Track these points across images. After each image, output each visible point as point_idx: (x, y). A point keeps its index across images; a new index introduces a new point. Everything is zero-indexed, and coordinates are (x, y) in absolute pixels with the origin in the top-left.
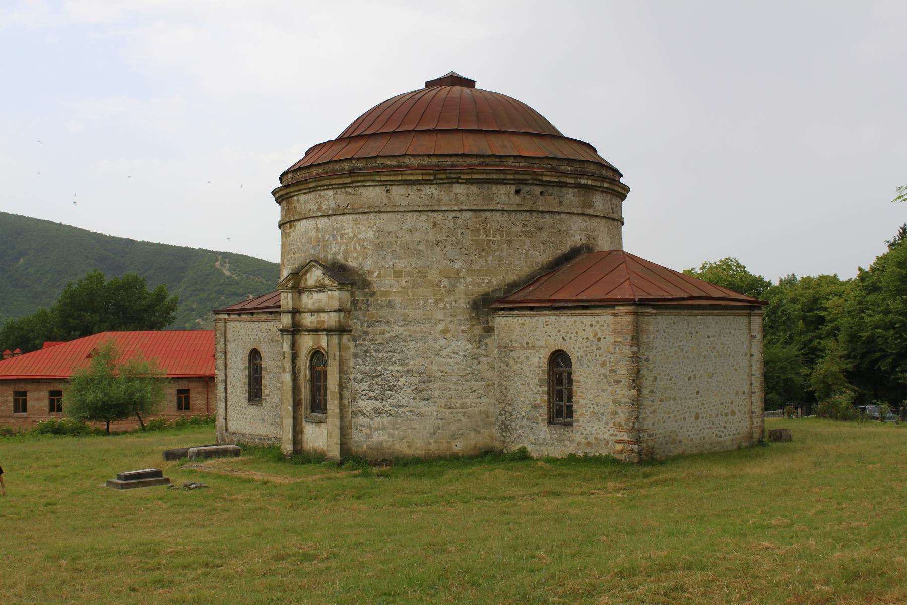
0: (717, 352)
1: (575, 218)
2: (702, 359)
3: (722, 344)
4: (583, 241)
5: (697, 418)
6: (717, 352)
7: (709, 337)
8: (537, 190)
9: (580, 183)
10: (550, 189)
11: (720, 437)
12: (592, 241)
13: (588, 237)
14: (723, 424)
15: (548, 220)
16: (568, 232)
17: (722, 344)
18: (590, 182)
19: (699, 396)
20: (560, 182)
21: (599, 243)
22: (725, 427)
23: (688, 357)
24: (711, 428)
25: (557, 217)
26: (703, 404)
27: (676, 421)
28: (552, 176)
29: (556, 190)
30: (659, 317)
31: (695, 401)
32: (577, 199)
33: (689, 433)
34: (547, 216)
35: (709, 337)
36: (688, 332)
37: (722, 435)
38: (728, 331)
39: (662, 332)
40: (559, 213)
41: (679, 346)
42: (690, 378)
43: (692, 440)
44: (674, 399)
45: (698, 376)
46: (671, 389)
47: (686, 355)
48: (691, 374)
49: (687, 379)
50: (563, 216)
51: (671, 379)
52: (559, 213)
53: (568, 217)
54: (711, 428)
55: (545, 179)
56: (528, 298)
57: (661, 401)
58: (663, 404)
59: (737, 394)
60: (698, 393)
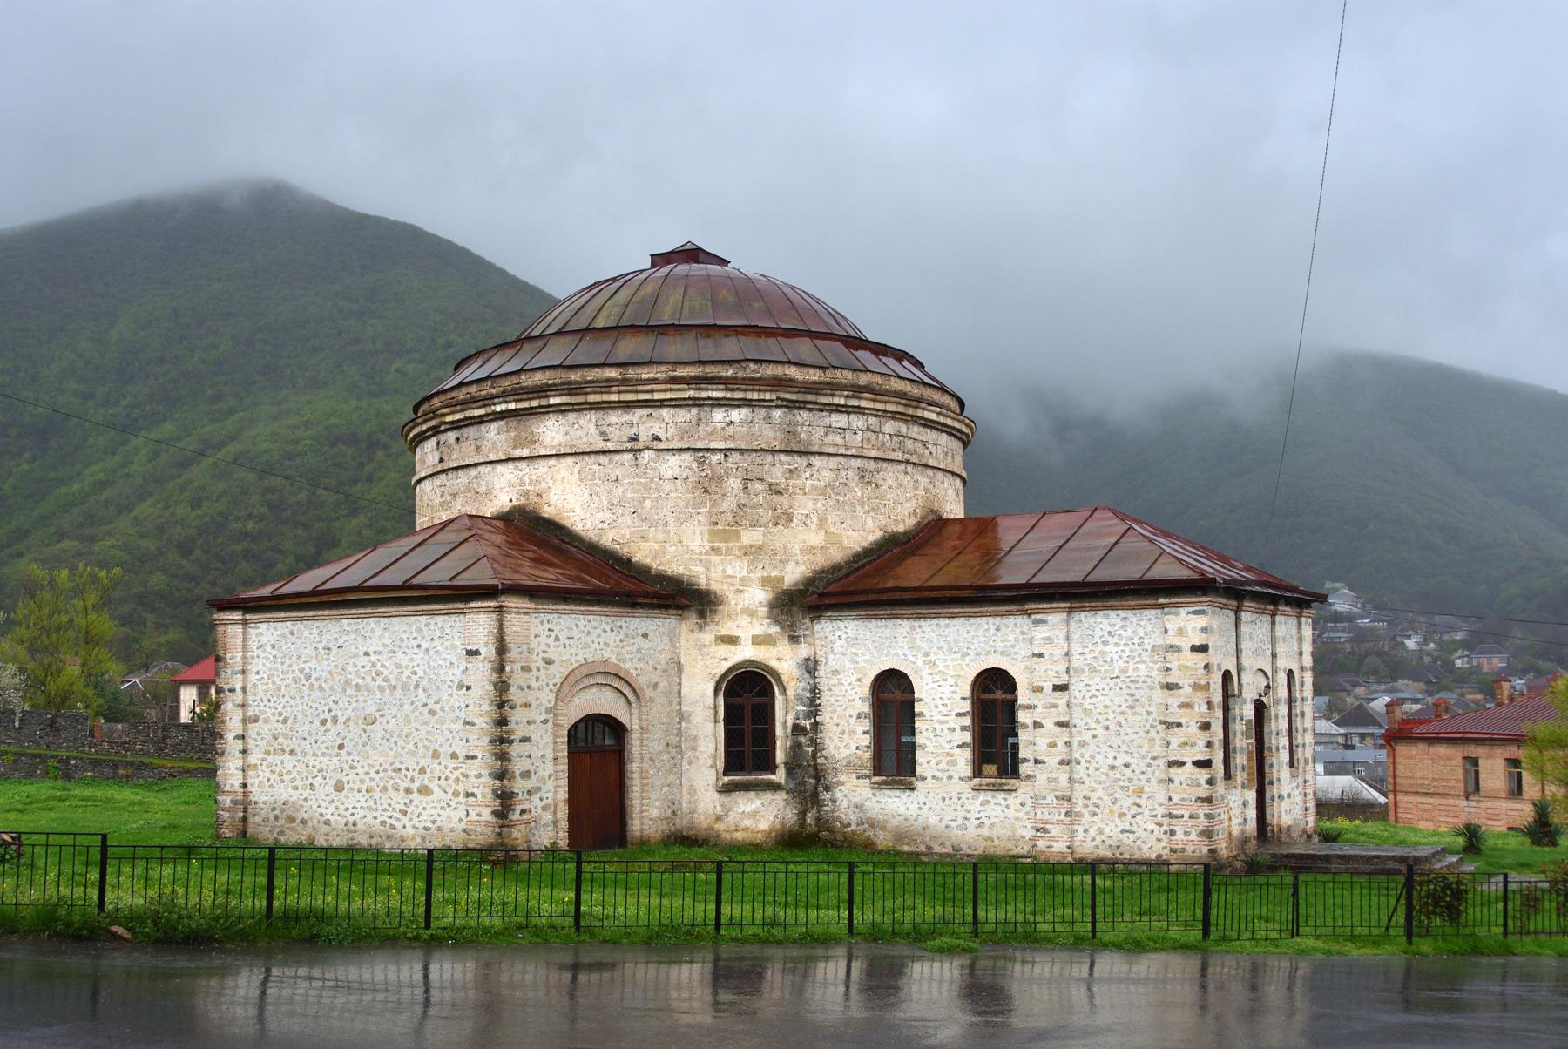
0: (386, 680)
1: (500, 468)
2: (349, 692)
3: (398, 666)
4: (515, 503)
5: (339, 787)
6: (386, 680)
7: (367, 654)
8: (452, 436)
9: (495, 413)
10: (466, 432)
11: (394, 828)
12: (536, 499)
13: (526, 494)
14: (399, 807)
15: (463, 478)
16: (488, 493)
17: (398, 666)
18: (512, 406)
19: (343, 753)
20: (466, 419)
21: (553, 497)
22: (405, 813)
23: (320, 688)
24: (369, 808)
25: (473, 472)
26: (352, 767)
27: (296, 788)
28: (452, 413)
29: (471, 432)
30: (263, 626)
31: (335, 760)
32: (503, 436)
33: (322, 810)
34: (461, 473)
35: (367, 654)
36: (320, 646)
37: (399, 825)
38: (415, 643)
39: (269, 649)
40: (476, 465)
41: (301, 671)
42: (323, 722)
43: (327, 823)
44: (292, 752)
45: (342, 719)
46: (286, 736)
47: (316, 685)
48: (327, 715)
49: (317, 723)
50: (481, 469)
51: (285, 721)
52: (476, 465)
53: (488, 468)
54: (369, 808)
55: (449, 419)
56: (861, 587)
57: (268, 753)
58: (270, 759)
59: (436, 755)
60: (341, 747)
